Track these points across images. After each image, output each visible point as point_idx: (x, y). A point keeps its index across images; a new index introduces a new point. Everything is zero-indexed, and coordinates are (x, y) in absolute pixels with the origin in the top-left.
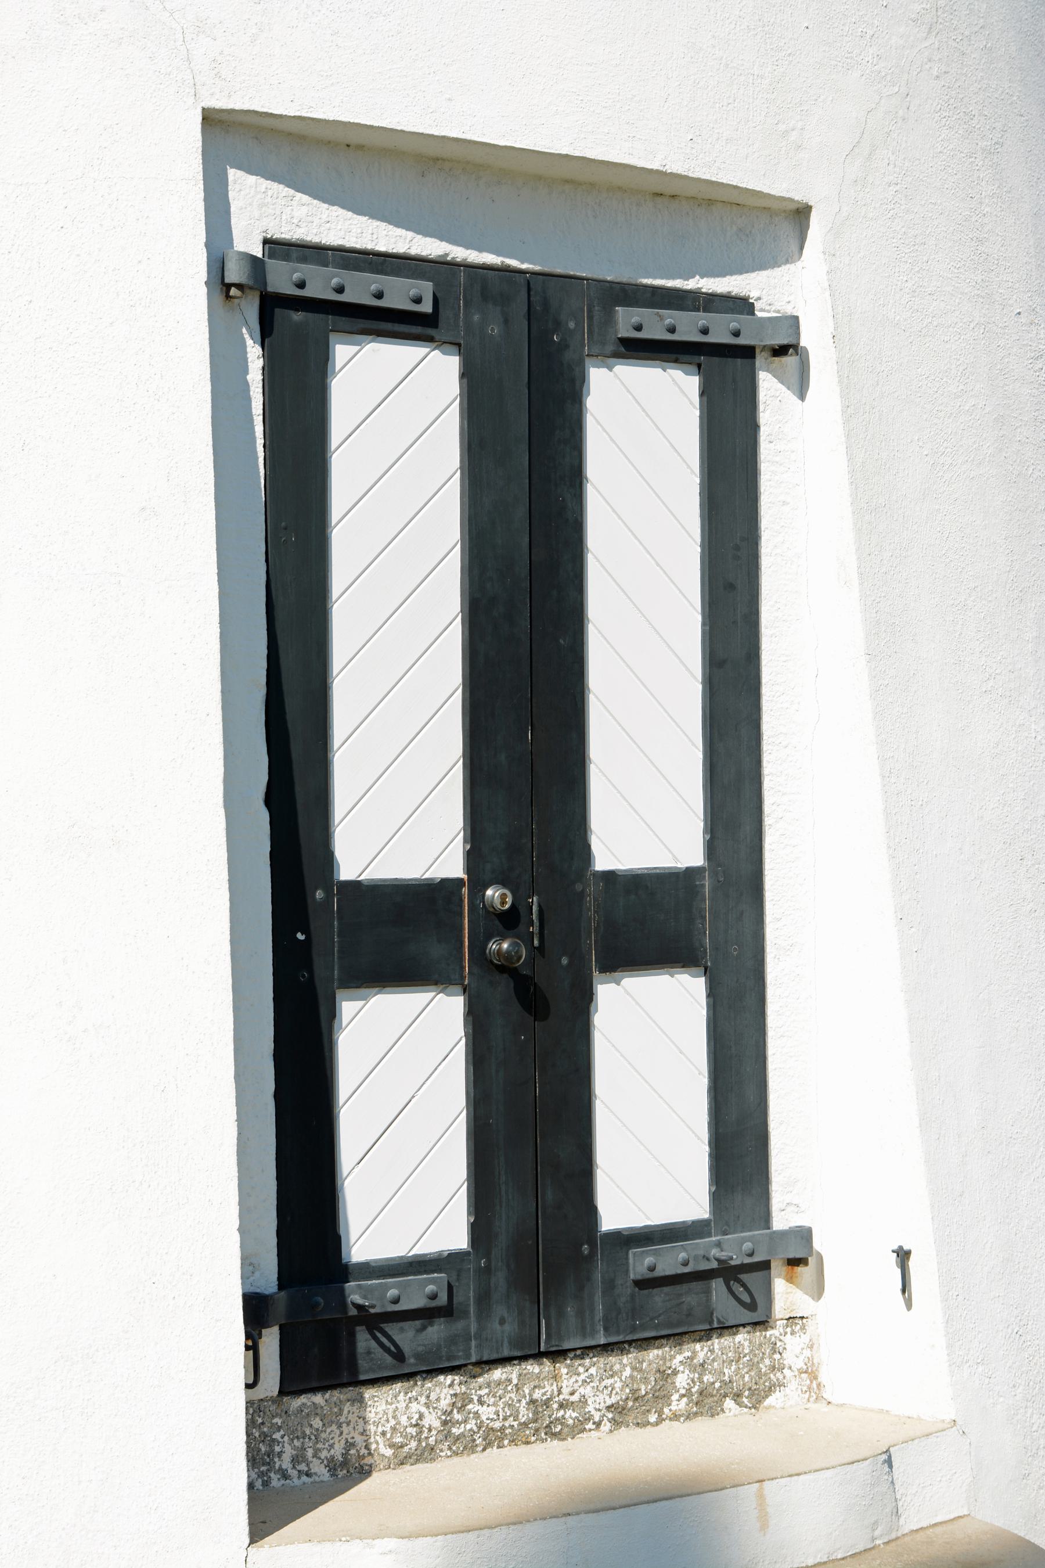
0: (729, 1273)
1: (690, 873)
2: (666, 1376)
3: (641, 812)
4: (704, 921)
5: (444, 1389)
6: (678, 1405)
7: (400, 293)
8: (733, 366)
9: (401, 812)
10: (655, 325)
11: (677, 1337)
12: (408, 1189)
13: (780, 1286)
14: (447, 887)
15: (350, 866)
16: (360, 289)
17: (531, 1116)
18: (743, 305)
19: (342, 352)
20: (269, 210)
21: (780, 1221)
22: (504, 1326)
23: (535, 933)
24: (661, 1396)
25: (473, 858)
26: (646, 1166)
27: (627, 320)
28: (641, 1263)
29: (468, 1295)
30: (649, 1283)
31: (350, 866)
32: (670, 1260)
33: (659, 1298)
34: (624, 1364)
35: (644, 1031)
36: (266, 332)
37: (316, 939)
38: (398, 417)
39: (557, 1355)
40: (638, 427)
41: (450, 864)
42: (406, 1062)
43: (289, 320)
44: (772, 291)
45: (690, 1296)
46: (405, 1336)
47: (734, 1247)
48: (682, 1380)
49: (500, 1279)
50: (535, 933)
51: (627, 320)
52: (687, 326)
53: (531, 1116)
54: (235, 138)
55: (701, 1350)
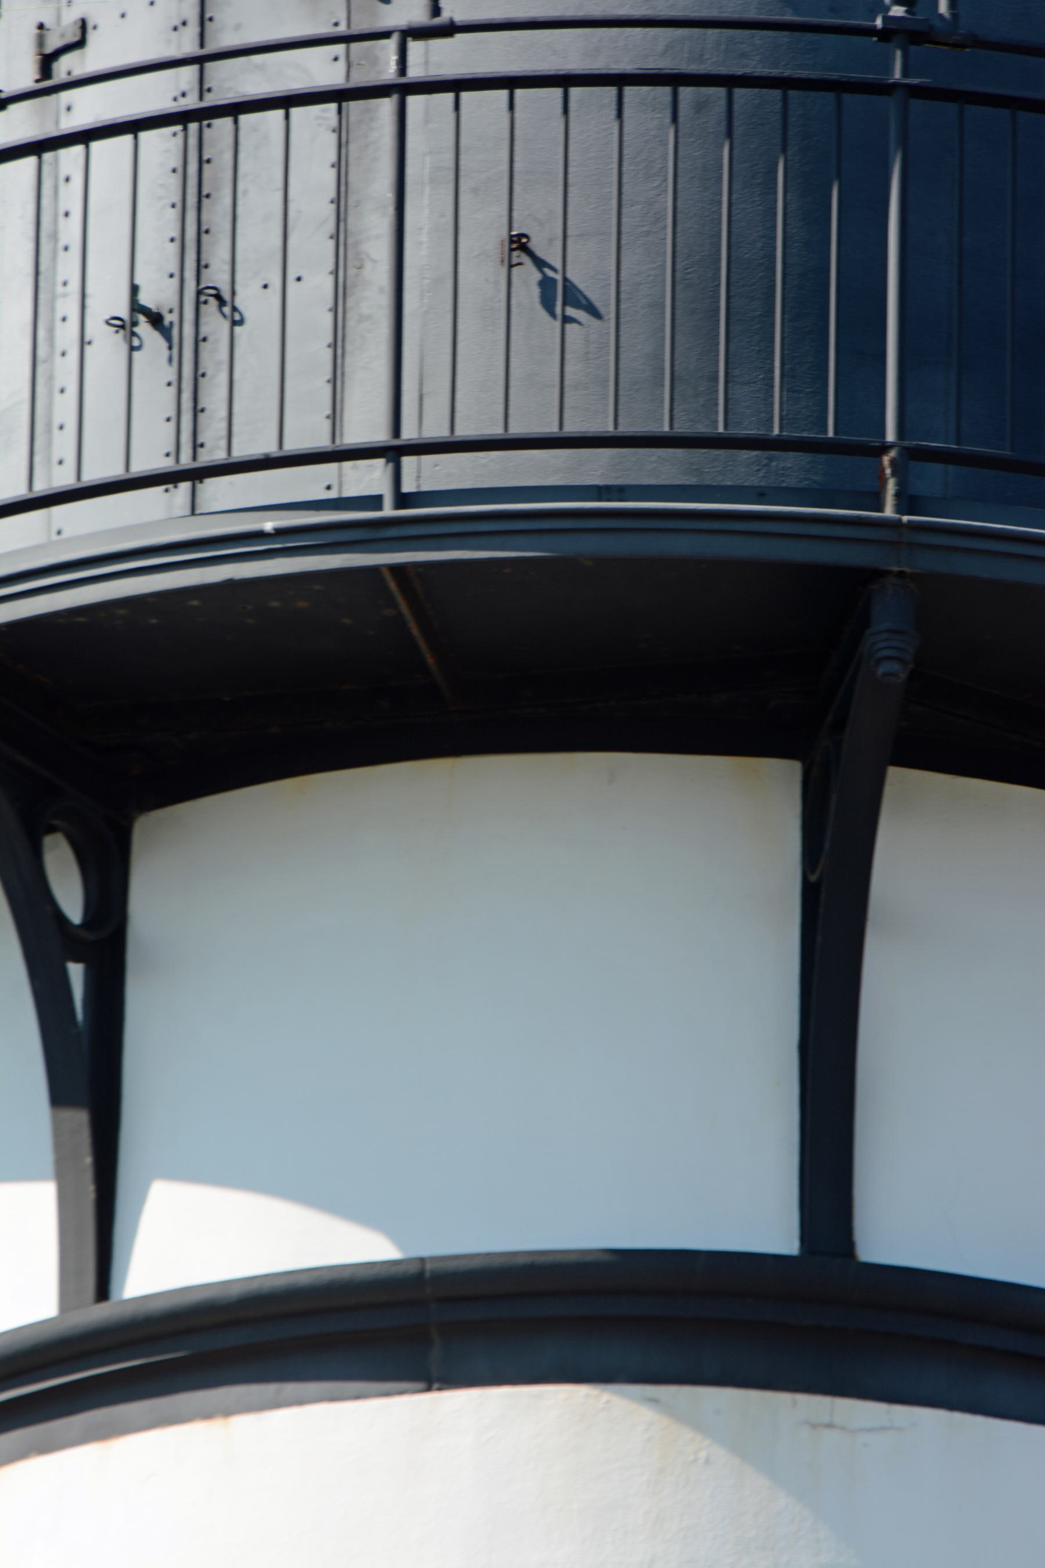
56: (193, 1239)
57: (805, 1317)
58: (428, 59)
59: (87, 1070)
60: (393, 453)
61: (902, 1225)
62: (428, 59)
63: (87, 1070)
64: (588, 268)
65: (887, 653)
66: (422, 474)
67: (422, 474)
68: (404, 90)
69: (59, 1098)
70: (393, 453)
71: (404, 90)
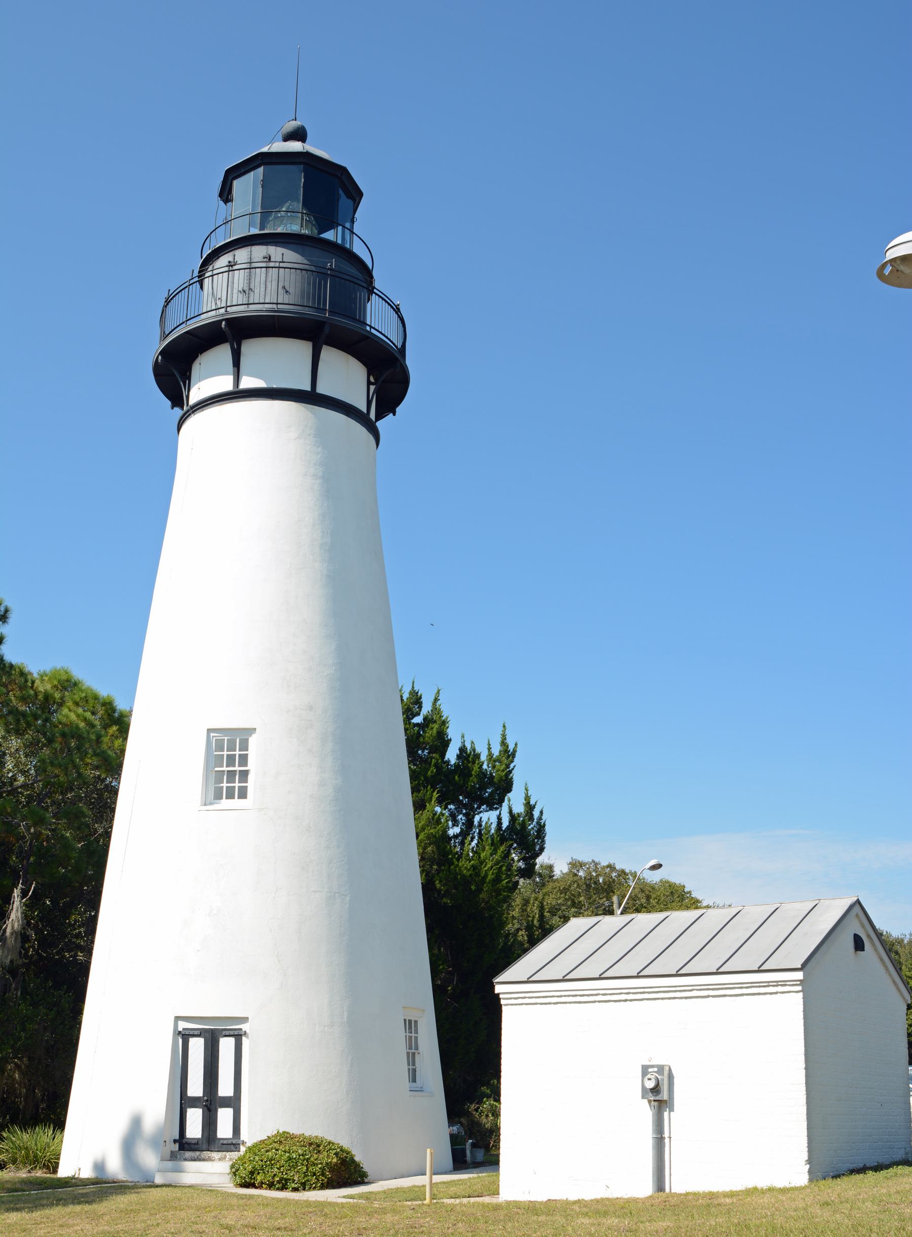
3: (225, 1089)
4: (234, 1102)
5: (198, 1153)
8: (238, 1037)
9: (196, 1088)
12: (194, 1130)
17: (210, 1123)
18: (241, 1029)
20: (182, 1025)
22: (205, 1146)
24: (225, 1157)
26: (224, 1130)
27: (224, 1033)
29: (200, 1142)
32: (225, 1142)
35: (224, 1116)
36: (183, 1038)
37: (186, 1102)
38: (197, 1046)
40: (226, 1046)
42: (195, 1117)
43: (185, 1036)
44: (244, 1027)
50: (211, 1103)
51: (224, 1033)
52: (232, 1033)
53: (210, 1123)
54: (178, 1019)
56: (247, 382)
57: (310, 397)
58: (282, 265)
59: (237, 363)
60: (277, 304)
61: (320, 390)
62: (282, 265)
63: (237, 363)
64: (292, 290)
65: (327, 330)
66: (280, 306)
67: (280, 306)
68: (279, 268)
69: (234, 366)
70: (277, 304)
71: (279, 268)
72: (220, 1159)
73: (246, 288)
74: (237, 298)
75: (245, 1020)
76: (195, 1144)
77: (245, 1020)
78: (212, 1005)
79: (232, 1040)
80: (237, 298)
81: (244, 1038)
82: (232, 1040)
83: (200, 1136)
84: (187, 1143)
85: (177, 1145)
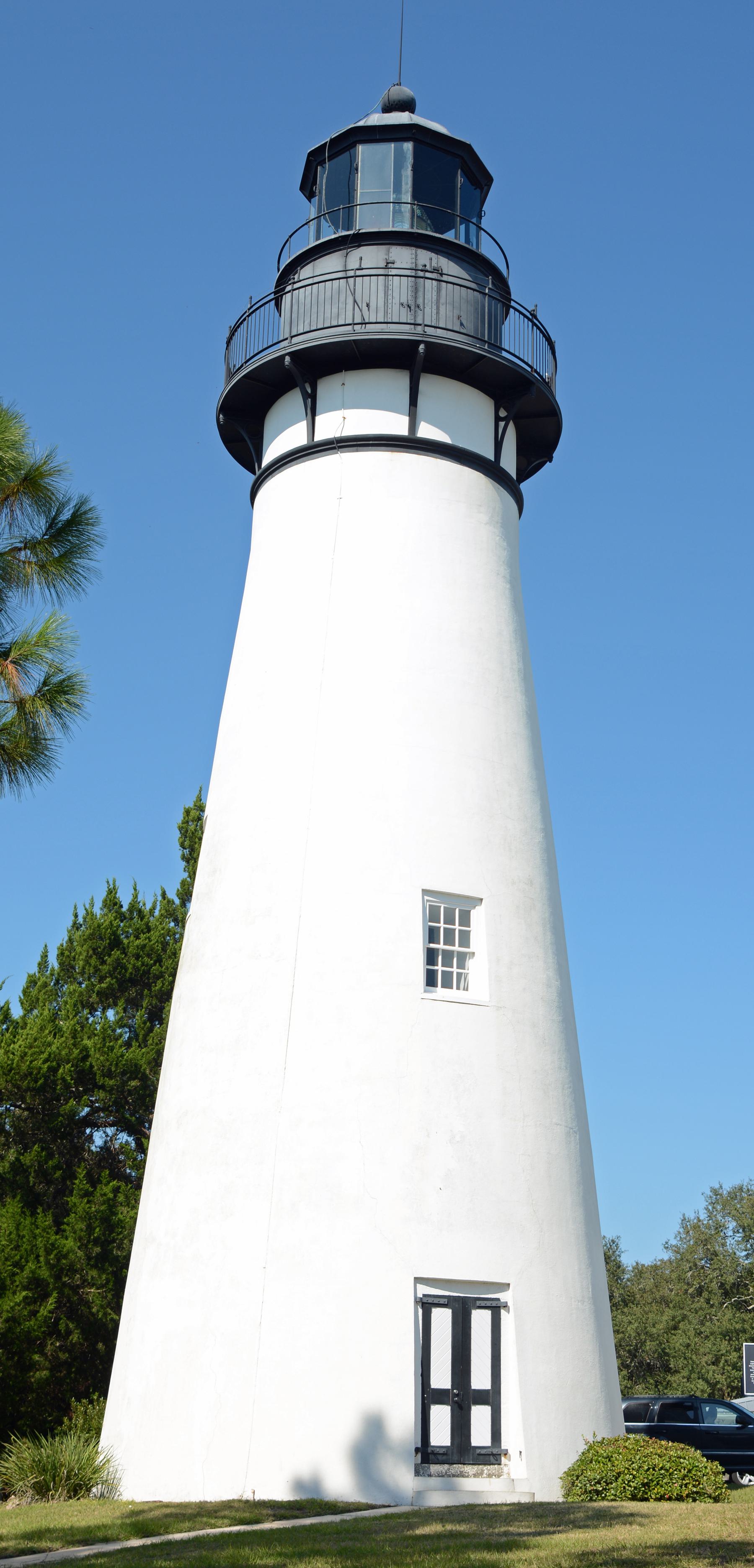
0: (493, 1455)
1: (488, 1390)
2: (483, 1471)
3: (480, 1380)
4: (491, 1398)
5: (446, 1466)
6: (484, 1475)
7: (442, 1301)
8: (496, 1309)
9: (441, 1379)
10: (483, 1303)
11: (485, 1464)
12: (441, 1435)
13: (503, 1458)
14: (448, 1390)
15: (433, 1386)
16: (436, 1301)
17: (461, 1426)
18: (498, 1300)
19: (433, 1310)
20: (424, 1290)
21: (503, 1448)
22: (456, 1458)
23: (462, 1398)
24: (482, 1474)
25: (452, 1385)
26: (480, 1436)
27: (478, 1303)
28: (478, 1451)
29: (450, 1452)
30: (479, 1454)
31: (433, 1386)
32: (483, 1452)
33: (481, 1457)
34: (476, 1467)
35: (480, 1415)
36: (422, 1307)
37: (428, 1397)
38: (442, 1319)
39: (464, 1464)
40: (480, 1320)
41: (450, 1387)
43: (426, 1305)
44: (503, 1297)
45: (487, 1458)
46: (440, 1457)
47: (495, 1451)
48: (485, 1472)
49: (455, 1451)
50: (462, 1398)
51: (478, 1303)
52: (488, 1304)
53: (461, 1426)
54: (418, 1280)
55: (489, 1467)
72: (475, 1476)
73: (411, 303)
74: (399, 314)
75: (505, 1287)
76: (443, 1454)
77: (505, 1287)
78: (464, 1266)
79: (487, 1314)
80: (399, 314)
81: (503, 1312)
82: (487, 1314)
83: (449, 1444)
84: (433, 1453)
85: (419, 1455)
